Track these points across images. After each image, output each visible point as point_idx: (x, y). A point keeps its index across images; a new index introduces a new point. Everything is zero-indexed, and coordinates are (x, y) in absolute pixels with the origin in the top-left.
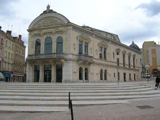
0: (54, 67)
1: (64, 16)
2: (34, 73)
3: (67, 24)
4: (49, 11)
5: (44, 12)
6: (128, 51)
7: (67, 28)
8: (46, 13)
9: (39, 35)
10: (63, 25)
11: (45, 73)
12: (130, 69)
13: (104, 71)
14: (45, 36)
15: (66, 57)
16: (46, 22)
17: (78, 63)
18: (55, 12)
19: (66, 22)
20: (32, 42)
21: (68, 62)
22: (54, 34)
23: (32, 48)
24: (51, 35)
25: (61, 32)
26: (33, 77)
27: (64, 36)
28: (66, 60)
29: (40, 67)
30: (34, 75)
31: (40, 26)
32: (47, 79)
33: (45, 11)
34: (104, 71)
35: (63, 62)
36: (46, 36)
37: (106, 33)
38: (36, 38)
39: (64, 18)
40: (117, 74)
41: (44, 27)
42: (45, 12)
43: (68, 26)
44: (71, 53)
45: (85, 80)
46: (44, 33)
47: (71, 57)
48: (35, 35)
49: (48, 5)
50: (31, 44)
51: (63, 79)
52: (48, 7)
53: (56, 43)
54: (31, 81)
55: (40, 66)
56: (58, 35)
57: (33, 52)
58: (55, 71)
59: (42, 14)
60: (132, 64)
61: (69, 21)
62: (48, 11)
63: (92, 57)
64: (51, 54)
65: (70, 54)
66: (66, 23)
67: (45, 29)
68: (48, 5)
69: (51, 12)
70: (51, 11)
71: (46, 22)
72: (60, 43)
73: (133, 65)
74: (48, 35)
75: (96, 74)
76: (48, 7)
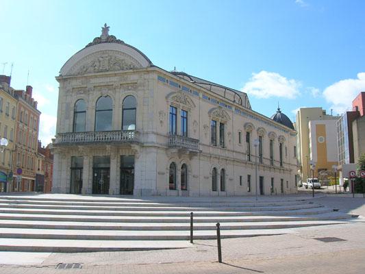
0: (115, 160)
1: (134, 48)
2: (69, 173)
4: (106, 39)
5: (95, 39)
6: (269, 129)
7: (146, 76)
8: (100, 43)
9: (85, 90)
10: (134, 69)
11: (96, 175)
12: (271, 167)
13: (219, 171)
14: (96, 94)
15: (142, 139)
16: (100, 62)
17: (167, 154)
19: (145, 64)
20: (68, 105)
21: (148, 150)
22: (117, 90)
25: (135, 85)
26: (69, 182)
27: (139, 95)
28: (142, 145)
29: (85, 161)
30: (69, 177)
32: (100, 188)
34: (219, 171)
35: (136, 151)
37: (224, 90)
39: (143, 58)
40: (245, 179)
42: (97, 41)
44: (155, 131)
45: (180, 192)
47: (152, 139)
49: (105, 25)
50: (64, 109)
51: (135, 187)
53: (121, 109)
55: (85, 157)
58: (117, 171)
59: (90, 45)
60: (277, 157)
61: (150, 62)
62: (104, 38)
63: (196, 141)
65: (153, 133)
67: (96, 77)
68: (105, 25)
69: (112, 41)
70: (112, 39)
71: (100, 62)
72: (129, 110)
73: (279, 159)
74: (105, 92)
75: (205, 177)
76: (106, 29)
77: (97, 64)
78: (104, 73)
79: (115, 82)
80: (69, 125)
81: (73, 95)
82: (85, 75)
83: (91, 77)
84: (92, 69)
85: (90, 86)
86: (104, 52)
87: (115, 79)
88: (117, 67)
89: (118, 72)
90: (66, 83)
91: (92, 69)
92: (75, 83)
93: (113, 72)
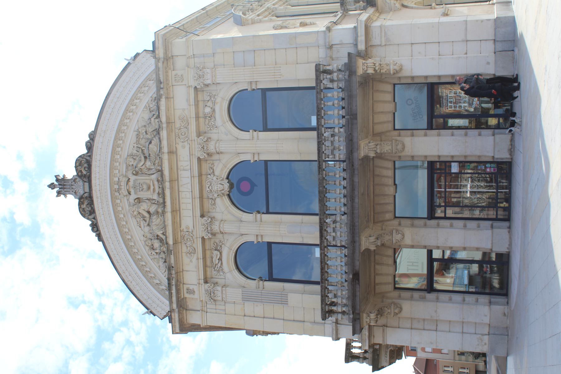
3: (157, 60)
5: (84, 216)
7: (180, 63)
10: (162, 86)
14: (223, 208)
18: (92, 136)
20: (246, 298)
23: (283, 301)
24: (217, 173)
31: (157, 244)
33: (80, 204)
36: (218, 201)
38: (228, 275)
41: (164, 213)
42: (87, 207)
43: (168, 59)
46: (202, 216)
48: (206, 282)
49: (52, 186)
52: (62, 186)
54: (498, 309)
56: (219, 122)
57: (312, 293)
59: (95, 227)
64: (320, 161)
66: (153, 61)
67: (176, 211)
68: (52, 186)
70: (84, 165)
76: (62, 186)
77: (144, 206)
78: (167, 185)
79: (191, 154)
80: (304, 292)
81: (220, 281)
82: (171, 242)
83: (176, 224)
84: (156, 220)
85: (200, 232)
86: (115, 191)
87: (183, 153)
88: (154, 147)
89: (165, 143)
90: (191, 304)
91: (156, 220)
92: (192, 273)
93: (165, 157)
